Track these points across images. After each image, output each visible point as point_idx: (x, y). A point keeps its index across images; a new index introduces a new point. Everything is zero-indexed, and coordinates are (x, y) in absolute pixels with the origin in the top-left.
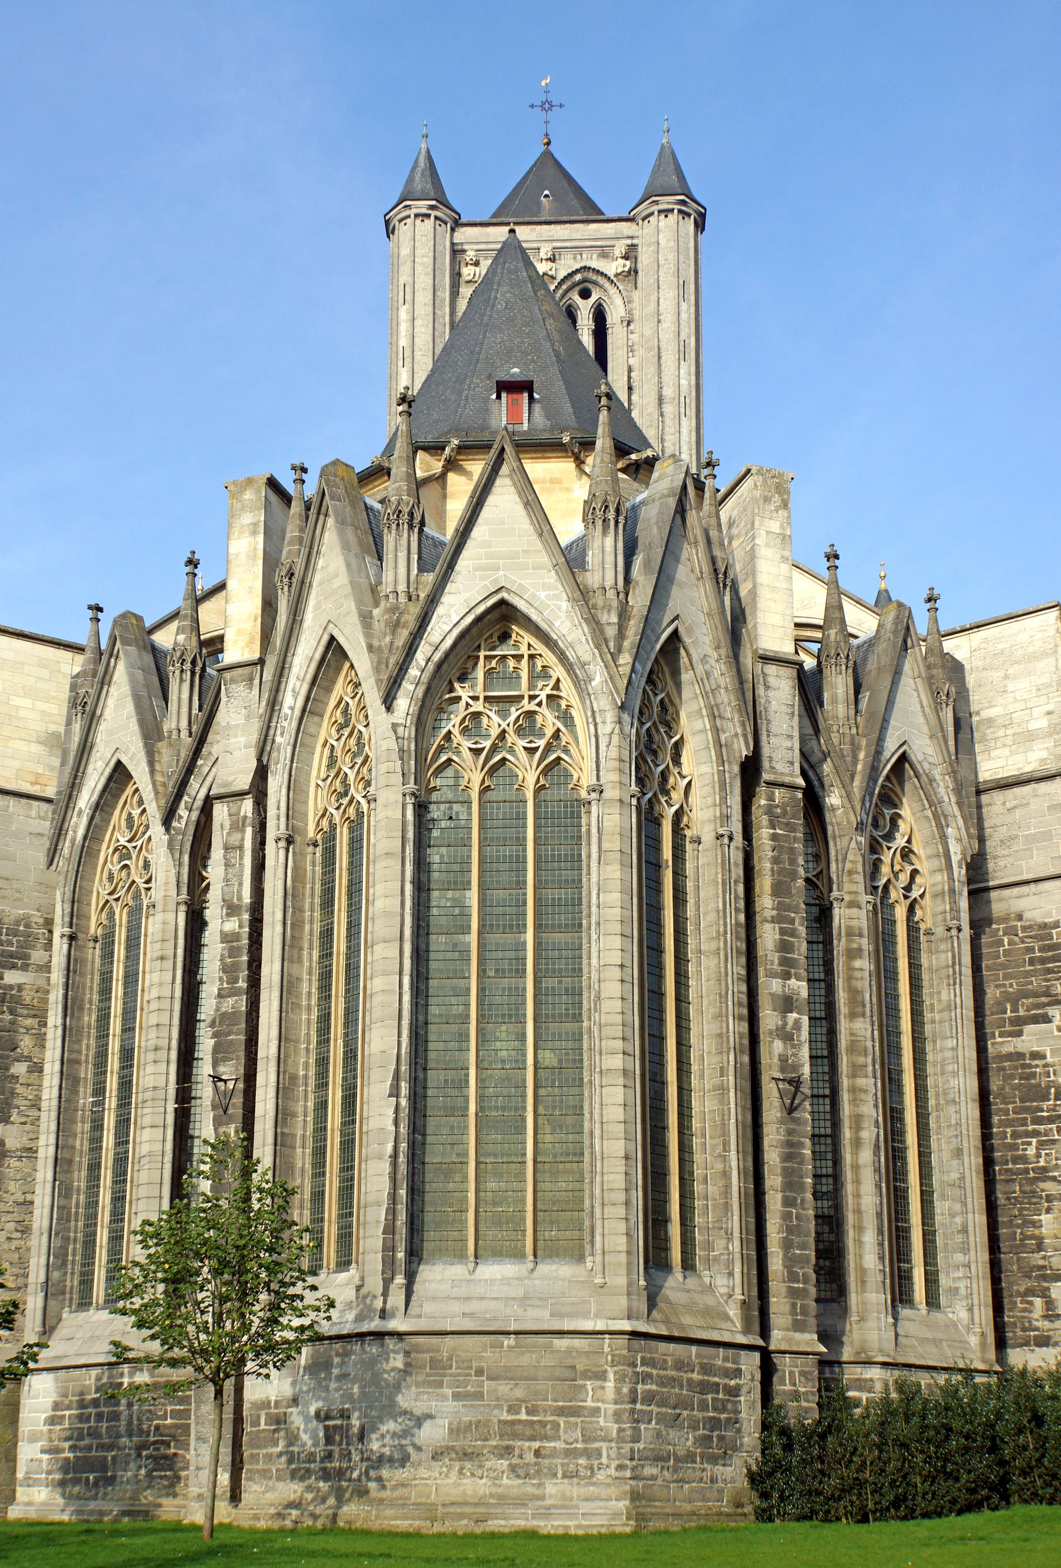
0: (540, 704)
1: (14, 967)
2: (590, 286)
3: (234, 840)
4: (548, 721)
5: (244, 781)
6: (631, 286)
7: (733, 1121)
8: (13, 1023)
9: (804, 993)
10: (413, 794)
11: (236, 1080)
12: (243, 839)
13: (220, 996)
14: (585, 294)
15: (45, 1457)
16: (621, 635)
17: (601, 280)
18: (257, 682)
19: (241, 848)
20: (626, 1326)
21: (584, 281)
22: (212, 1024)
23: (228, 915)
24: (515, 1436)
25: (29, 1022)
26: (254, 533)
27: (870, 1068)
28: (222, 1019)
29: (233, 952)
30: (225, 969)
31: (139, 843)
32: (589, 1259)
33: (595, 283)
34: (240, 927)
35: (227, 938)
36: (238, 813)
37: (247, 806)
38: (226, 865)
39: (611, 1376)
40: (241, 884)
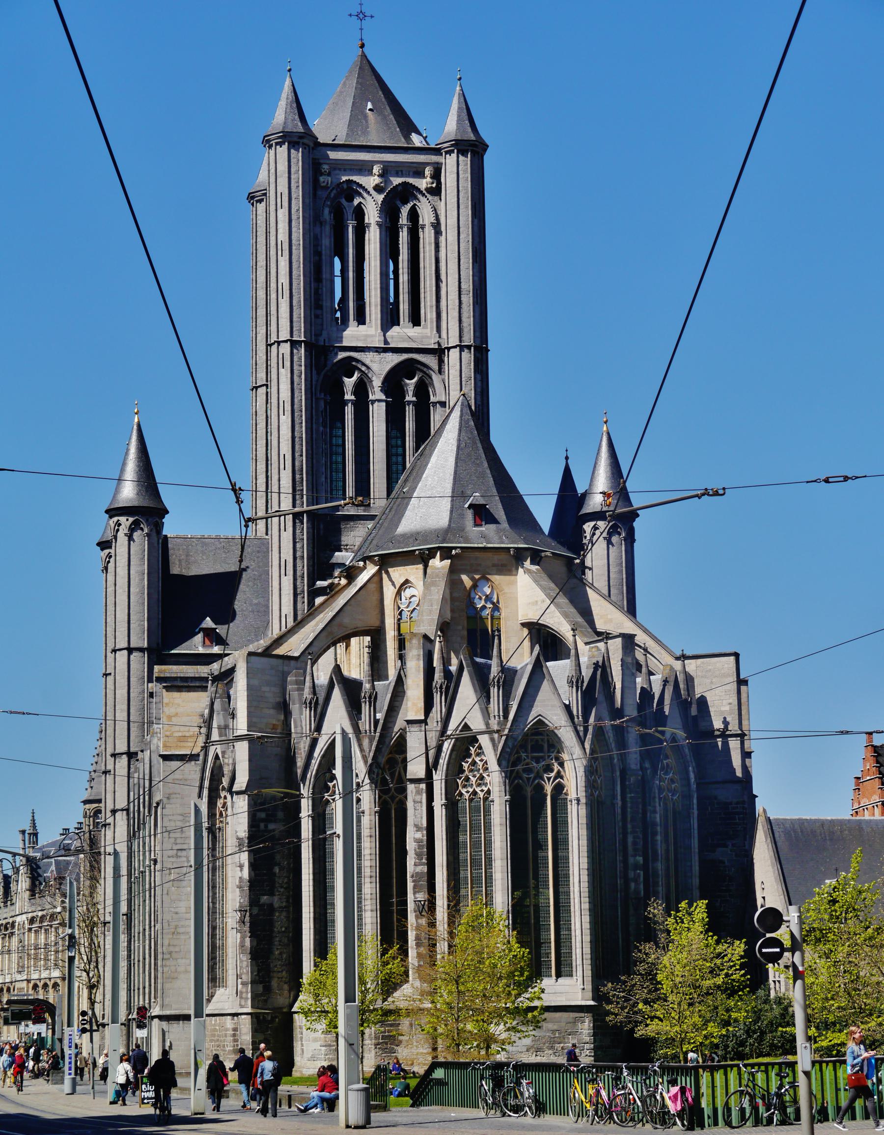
1: (271, 821)
3: (418, 798)
4: (556, 767)
5: (422, 774)
7: (619, 919)
9: (642, 862)
11: (425, 901)
13: (415, 865)
14: (405, 202)
15: (324, 1048)
16: (585, 735)
18: (423, 728)
19: (421, 802)
20: (592, 1003)
22: (412, 877)
24: (555, 1042)
26: (418, 659)
27: (660, 883)
28: (417, 876)
29: (420, 847)
32: (575, 978)
34: (423, 836)
35: (417, 841)
36: (419, 787)
38: (415, 809)
39: (587, 1020)
40: (422, 818)
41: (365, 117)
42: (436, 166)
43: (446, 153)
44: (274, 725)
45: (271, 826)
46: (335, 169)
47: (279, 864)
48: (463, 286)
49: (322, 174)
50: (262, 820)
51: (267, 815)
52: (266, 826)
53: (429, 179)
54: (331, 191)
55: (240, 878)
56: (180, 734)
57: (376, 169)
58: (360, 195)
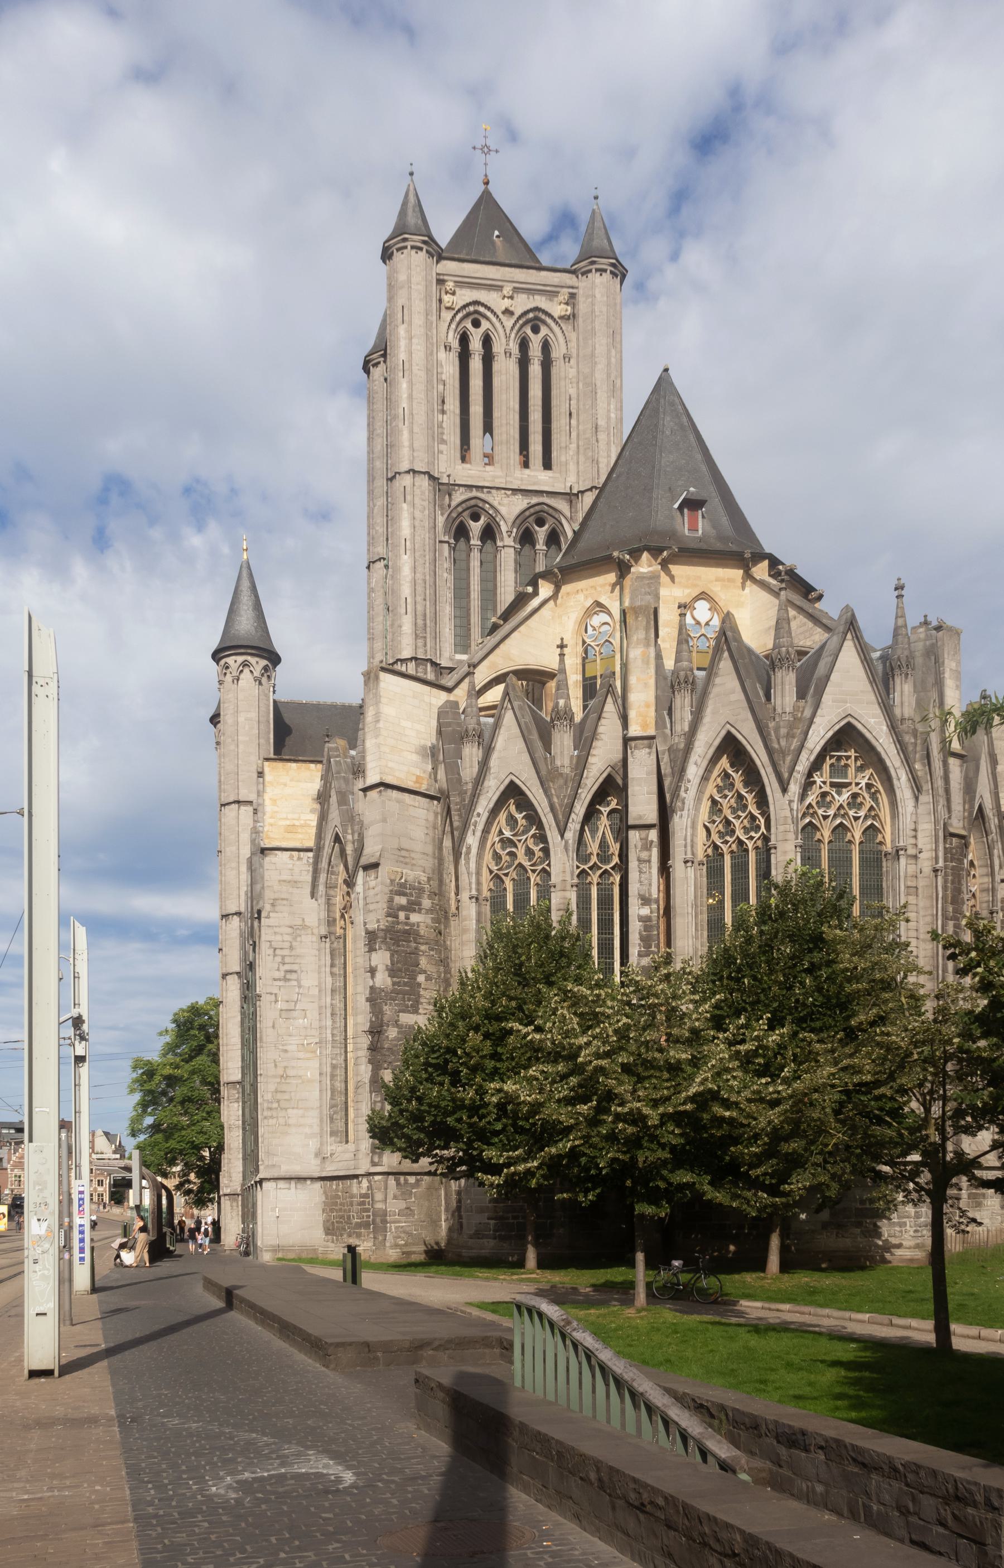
0: (861, 789)
1: (414, 911)
2: (540, 324)
3: (644, 855)
6: (570, 327)
8: (416, 948)
10: (801, 846)
12: (650, 856)
14: (536, 330)
17: (549, 321)
19: (649, 861)
21: (536, 318)
23: (642, 904)
25: (423, 948)
30: (642, 938)
31: (524, 837)
33: (544, 322)
34: (651, 912)
35: (641, 919)
37: (653, 835)
38: (640, 872)
40: (650, 885)
41: (493, 243)
42: (571, 290)
43: (583, 274)
44: (418, 777)
45: (415, 918)
46: (461, 287)
47: (425, 972)
48: (602, 423)
49: (447, 293)
50: (402, 908)
51: (408, 900)
52: (407, 918)
53: (563, 306)
54: (459, 311)
55: (371, 988)
56: (288, 823)
57: (507, 290)
58: (488, 319)
